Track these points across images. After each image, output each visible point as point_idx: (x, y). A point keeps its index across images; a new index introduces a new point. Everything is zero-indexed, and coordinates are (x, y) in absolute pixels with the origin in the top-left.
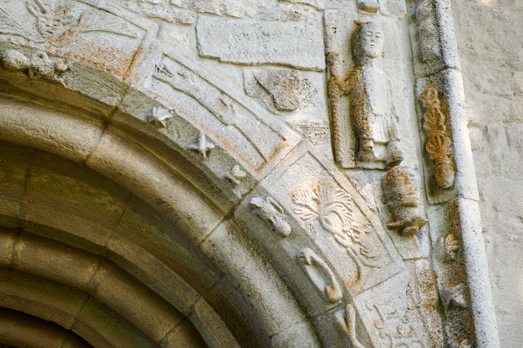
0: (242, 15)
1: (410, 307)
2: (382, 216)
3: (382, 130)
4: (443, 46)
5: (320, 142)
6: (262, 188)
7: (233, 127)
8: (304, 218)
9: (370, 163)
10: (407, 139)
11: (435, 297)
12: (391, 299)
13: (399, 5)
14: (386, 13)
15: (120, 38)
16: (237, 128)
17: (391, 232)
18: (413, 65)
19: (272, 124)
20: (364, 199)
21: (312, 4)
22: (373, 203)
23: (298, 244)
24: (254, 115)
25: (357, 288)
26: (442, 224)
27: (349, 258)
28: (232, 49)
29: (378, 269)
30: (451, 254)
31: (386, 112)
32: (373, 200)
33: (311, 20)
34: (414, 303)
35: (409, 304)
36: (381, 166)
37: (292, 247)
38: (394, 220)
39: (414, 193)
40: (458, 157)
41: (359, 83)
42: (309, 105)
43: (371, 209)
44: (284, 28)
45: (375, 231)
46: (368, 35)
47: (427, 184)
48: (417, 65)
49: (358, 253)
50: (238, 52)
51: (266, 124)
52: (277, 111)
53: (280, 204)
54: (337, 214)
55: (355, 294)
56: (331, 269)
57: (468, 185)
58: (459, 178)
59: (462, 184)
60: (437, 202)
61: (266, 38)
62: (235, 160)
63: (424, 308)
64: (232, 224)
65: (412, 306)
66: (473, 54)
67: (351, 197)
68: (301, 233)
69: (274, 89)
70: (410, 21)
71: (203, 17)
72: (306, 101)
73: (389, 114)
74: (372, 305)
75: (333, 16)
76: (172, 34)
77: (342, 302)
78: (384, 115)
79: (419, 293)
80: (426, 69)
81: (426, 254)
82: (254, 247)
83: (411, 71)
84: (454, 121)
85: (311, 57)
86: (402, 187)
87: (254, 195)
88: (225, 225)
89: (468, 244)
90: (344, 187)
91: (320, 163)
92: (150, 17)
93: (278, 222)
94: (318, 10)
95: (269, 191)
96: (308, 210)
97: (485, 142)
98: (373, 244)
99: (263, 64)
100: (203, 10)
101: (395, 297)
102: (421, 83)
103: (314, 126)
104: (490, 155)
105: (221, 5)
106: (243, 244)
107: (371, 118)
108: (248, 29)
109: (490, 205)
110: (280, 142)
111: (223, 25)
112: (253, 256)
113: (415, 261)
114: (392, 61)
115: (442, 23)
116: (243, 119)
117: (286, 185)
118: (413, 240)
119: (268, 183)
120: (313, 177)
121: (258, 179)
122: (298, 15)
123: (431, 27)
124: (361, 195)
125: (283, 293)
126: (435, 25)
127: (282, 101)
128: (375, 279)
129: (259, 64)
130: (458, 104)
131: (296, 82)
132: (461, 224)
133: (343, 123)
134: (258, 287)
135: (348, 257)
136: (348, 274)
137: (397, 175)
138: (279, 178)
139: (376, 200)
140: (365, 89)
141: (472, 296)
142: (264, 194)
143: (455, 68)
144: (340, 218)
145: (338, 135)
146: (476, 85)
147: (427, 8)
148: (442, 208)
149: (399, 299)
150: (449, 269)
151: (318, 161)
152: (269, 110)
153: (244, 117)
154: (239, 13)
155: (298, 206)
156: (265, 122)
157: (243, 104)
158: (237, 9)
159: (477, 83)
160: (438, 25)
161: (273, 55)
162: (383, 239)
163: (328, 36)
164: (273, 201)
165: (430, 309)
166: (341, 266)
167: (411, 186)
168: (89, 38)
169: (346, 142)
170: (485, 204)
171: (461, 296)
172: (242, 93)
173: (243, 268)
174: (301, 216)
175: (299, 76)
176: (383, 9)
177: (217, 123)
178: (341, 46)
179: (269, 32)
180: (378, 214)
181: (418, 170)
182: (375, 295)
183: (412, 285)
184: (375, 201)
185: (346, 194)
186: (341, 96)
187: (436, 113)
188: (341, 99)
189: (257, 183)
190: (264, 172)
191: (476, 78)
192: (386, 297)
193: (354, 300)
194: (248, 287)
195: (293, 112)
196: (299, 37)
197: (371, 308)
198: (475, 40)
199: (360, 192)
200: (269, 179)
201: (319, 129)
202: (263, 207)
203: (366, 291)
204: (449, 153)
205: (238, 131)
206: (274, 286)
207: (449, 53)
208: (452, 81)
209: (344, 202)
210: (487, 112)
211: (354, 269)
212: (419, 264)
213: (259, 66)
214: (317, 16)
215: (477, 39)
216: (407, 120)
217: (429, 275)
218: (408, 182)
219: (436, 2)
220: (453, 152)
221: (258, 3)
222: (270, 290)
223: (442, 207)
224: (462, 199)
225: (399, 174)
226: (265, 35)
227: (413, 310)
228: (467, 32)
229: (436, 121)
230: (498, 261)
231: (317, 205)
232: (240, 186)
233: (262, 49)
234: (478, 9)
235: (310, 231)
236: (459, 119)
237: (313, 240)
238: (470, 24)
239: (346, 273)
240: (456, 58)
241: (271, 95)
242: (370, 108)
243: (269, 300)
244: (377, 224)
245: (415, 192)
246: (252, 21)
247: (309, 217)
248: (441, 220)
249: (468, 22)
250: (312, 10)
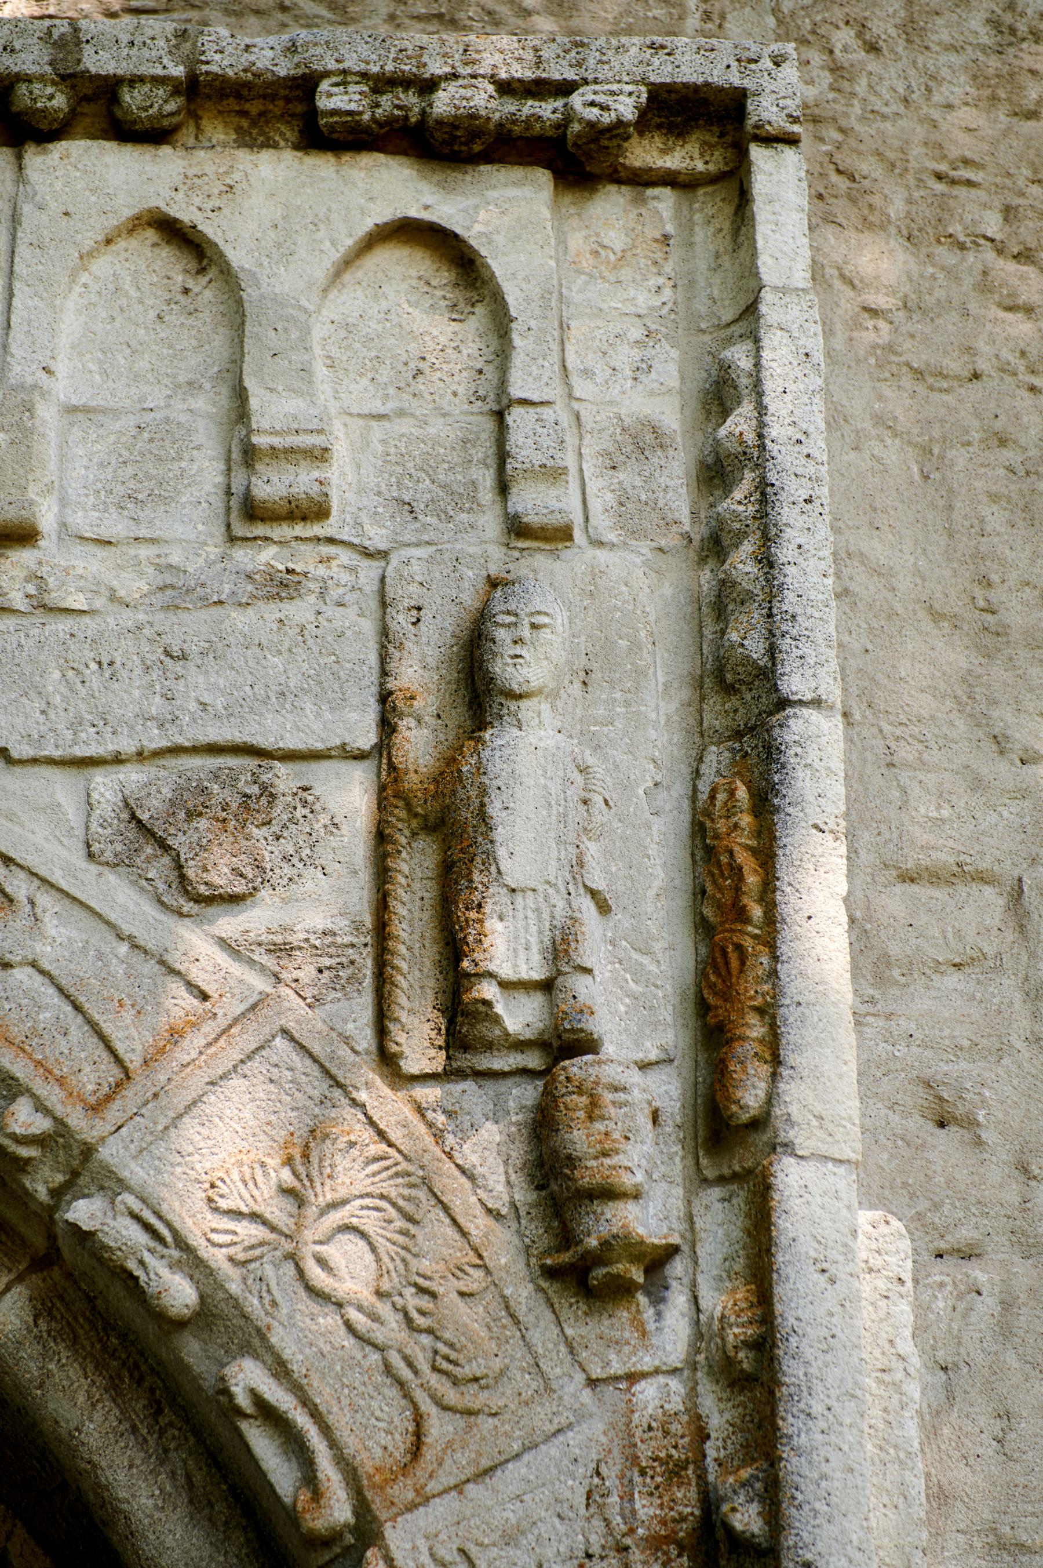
0: (99, 603)
1: (595, 1549)
2: (527, 1233)
3: (534, 941)
4: (777, 632)
5: (333, 995)
6: (103, 1168)
7: (29, 970)
8: (241, 1256)
9: (495, 1053)
10: (645, 960)
11: (689, 1510)
12: (525, 1524)
13: (661, 503)
14: (612, 537)
16: (42, 972)
17: (551, 1288)
18: (702, 699)
19: (166, 950)
20: (469, 1178)
21: (345, 538)
22: (500, 1188)
23: (222, 1346)
24: (108, 923)
25: (402, 1491)
26: (737, 1247)
27: (392, 1385)
28: (53, 717)
29: (490, 1420)
30: (741, 1355)
31: (552, 879)
32: (503, 1178)
33: (341, 591)
34: (611, 1534)
35: (593, 1538)
36: (533, 1060)
37: (208, 1357)
39: (617, 1152)
40: (789, 1014)
41: (464, 787)
42: (304, 872)
43: (489, 1211)
44: (240, 625)
45: (496, 1285)
46: (503, 625)
47: (700, 1109)
48: (711, 702)
49: (424, 1367)
50: (72, 724)
51: (146, 952)
52: (191, 904)
53: (160, 1217)
54: (363, 1235)
55: (395, 1510)
56: (320, 1428)
57: (819, 1108)
58: (782, 1086)
59: (794, 1109)
60: (726, 1172)
61: (178, 667)
62: (17, 1080)
63: (642, 1552)
64: (55, 1284)
65: (603, 1547)
66: (993, 629)
67: (421, 1173)
68: (228, 1310)
69: (185, 833)
70: (704, 554)
72: (295, 860)
73: (561, 884)
74: (455, 1547)
75: (416, 567)
77: (353, 1541)
78: (540, 888)
79: (631, 1500)
80: (736, 711)
81: (673, 1357)
82: (123, 1356)
83: (692, 721)
84: (788, 889)
85: (327, 716)
86: (575, 1132)
87: (86, 1191)
88: (28, 1288)
89: (792, 1321)
90: (398, 1143)
91: (322, 1066)
93: (152, 1276)
94: (367, 554)
95: (125, 1174)
96: (261, 1228)
97: (1010, 935)
98: (484, 1333)
99: (158, 754)
101: (543, 1514)
102: (716, 758)
103: (317, 943)
104: (1026, 979)
105: (27, 580)
106: (83, 1348)
107: (495, 900)
108: (115, 645)
109: (1005, 1157)
110: (188, 1008)
111: (31, 642)
112: (116, 1388)
113: (632, 1384)
114: (618, 695)
115: (785, 553)
116: (69, 939)
117: (191, 1149)
118: (634, 1309)
119: (126, 1148)
120: (294, 1114)
121: (90, 1136)
122: (296, 578)
123: (748, 569)
124: (457, 1166)
125: (207, 1511)
126: (760, 562)
127: (205, 869)
128: (473, 1455)
129: (146, 754)
130: (816, 827)
131: (264, 801)
132: (773, 1249)
133: (417, 923)
134: (122, 1494)
135: (388, 1381)
136: (378, 1444)
137: (564, 1090)
138: (166, 1128)
139: (513, 1177)
140: (483, 805)
141: (784, 1505)
142: (113, 1185)
144: (373, 1249)
145: (393, 968)
146: (995, 737)
147: (741, 508)
148: (741, 1193)
149: (557, 1521)
150: (745, 1408)
151: (315, 1060)
152: (162, 903)
153: (74, 934)
154: (89, 595)
155: (225, 1220)
156: (142, 943)
157: (72, 891)
158: (82, 583)
159: (996, 731)
160: (767, 562)
161: (194, 720)
162: (521, 1312)
163: (391, 637)
164: (136, 1205)
165: (665, 1553)
166: (359, 1416)
167: (612, 1125)
169: (422, 987)
170: (986, 1156)
171: (754, 1508)
172: (78, 859)
173: (77, 1429)
174: (232, 1250)
175: (277, 781)
176: (603, 524)
178: (434, 664)
179: (185, 646)
180: (515, 1225)
181: (676, 1063)
182: (468, 1513)
183: (611, 1473)
184: (508, 1182)
185: (404, 1166)
186: (414, 834)
187: (730, 865)
188: (414, 845)
189: (88, 1151)
190: (114, 1113)
191: (995, 714)
192: (511, 1514)
193: (388, 1532)
194: (96, 1494)
195: (248, 902)
196: (290, 650)
197: (448, 1558)
198: (1003, 582)
199: (455, 1154)
200: (131, 1134)
201: (332, 950)
202: (102, 1231)
203: (437, 1500)
204: (758, 1002)
205: (47, 981)
206: (175, 1487)
207: (800, 653)
208: (799, 750)
209: (393, 1194)
210: (1030, 829)
211: (404, 1423)
212: (648, 1392)
213: (146, 763)
214: (362, 574)
215: (1013, 576)
216: (651, 893)
217: (680, 1433)
218: (597, 1112)
219: (767, 485)
220: (774, 997)
221: (159, 556)
222: (160, 1503)
223: (743, 1188)
224: (788, 1161)
225: (570, 1089)
226: (172, 657)
227: (602, 1558)
228: (978, 557)
229: (732, 893)
230: (1011, 1359)
231: (295, 1210)
232: (42, 1162)
233: (156, 706)
234: (1028, 473)
235: (256, 1302)
236: (810, 880)
237: (264, 1330)
238: (989, 529)
239: (370, 1438)
240: (825, 669)
241: (174, 853)
242: (493, 869)
243: (152, 1537)
244: (503, 1261)
245: (623, 1146)
246: (129, 618)
247: (257, 1252)
248: (737, 1234)
249: (982, 520)
250: (345, 556)
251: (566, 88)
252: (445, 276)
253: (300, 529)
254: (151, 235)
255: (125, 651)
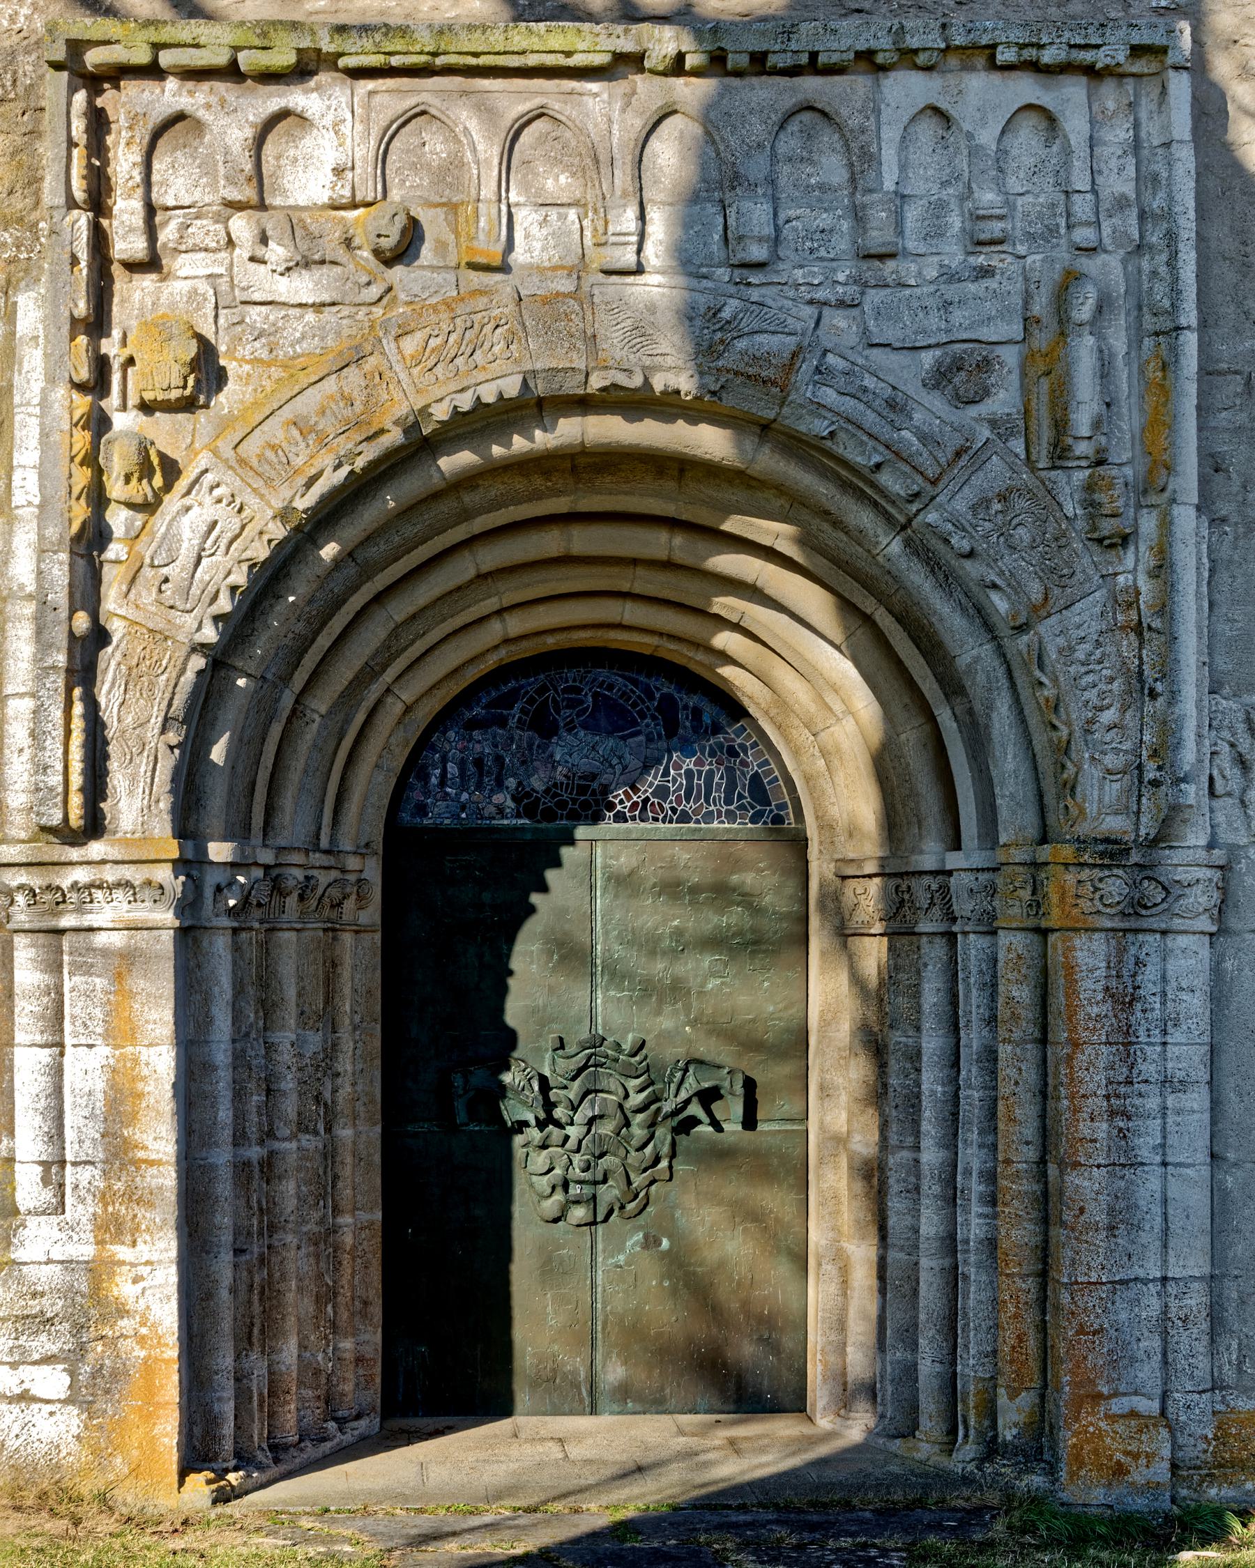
15: (776, 339)
38: (1094, 529)
71: (873, 292)
76: (835, 322)
92: (811, 302)
100: (873, 282)
143: (1188, 328)
168: (741, 344)
177: (888, 428)
183: (1109, 605)
190: (941, 485)
192: (1077, 619)
211: (1042, 589)
212: (1121, 579)
250: (1009, 259)
251: (1097, 47)
252: (1044, 124)
253: (993, 248)
254: (929, 112)
255: (930, 302)
